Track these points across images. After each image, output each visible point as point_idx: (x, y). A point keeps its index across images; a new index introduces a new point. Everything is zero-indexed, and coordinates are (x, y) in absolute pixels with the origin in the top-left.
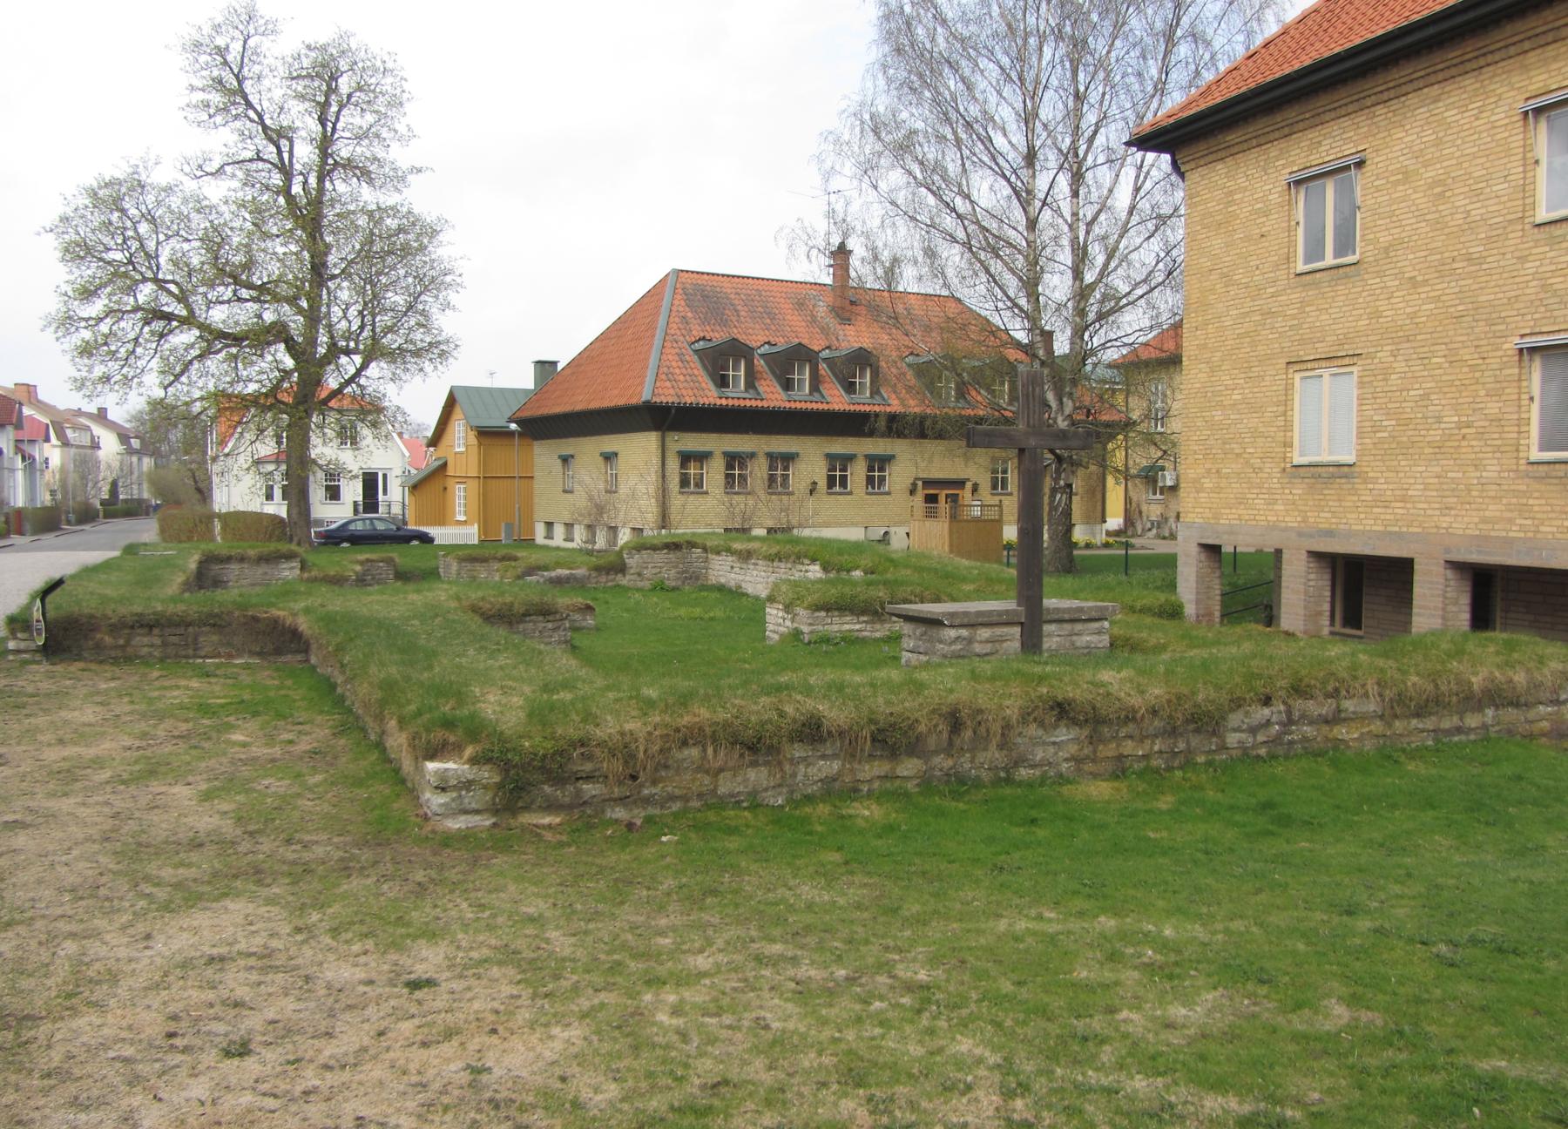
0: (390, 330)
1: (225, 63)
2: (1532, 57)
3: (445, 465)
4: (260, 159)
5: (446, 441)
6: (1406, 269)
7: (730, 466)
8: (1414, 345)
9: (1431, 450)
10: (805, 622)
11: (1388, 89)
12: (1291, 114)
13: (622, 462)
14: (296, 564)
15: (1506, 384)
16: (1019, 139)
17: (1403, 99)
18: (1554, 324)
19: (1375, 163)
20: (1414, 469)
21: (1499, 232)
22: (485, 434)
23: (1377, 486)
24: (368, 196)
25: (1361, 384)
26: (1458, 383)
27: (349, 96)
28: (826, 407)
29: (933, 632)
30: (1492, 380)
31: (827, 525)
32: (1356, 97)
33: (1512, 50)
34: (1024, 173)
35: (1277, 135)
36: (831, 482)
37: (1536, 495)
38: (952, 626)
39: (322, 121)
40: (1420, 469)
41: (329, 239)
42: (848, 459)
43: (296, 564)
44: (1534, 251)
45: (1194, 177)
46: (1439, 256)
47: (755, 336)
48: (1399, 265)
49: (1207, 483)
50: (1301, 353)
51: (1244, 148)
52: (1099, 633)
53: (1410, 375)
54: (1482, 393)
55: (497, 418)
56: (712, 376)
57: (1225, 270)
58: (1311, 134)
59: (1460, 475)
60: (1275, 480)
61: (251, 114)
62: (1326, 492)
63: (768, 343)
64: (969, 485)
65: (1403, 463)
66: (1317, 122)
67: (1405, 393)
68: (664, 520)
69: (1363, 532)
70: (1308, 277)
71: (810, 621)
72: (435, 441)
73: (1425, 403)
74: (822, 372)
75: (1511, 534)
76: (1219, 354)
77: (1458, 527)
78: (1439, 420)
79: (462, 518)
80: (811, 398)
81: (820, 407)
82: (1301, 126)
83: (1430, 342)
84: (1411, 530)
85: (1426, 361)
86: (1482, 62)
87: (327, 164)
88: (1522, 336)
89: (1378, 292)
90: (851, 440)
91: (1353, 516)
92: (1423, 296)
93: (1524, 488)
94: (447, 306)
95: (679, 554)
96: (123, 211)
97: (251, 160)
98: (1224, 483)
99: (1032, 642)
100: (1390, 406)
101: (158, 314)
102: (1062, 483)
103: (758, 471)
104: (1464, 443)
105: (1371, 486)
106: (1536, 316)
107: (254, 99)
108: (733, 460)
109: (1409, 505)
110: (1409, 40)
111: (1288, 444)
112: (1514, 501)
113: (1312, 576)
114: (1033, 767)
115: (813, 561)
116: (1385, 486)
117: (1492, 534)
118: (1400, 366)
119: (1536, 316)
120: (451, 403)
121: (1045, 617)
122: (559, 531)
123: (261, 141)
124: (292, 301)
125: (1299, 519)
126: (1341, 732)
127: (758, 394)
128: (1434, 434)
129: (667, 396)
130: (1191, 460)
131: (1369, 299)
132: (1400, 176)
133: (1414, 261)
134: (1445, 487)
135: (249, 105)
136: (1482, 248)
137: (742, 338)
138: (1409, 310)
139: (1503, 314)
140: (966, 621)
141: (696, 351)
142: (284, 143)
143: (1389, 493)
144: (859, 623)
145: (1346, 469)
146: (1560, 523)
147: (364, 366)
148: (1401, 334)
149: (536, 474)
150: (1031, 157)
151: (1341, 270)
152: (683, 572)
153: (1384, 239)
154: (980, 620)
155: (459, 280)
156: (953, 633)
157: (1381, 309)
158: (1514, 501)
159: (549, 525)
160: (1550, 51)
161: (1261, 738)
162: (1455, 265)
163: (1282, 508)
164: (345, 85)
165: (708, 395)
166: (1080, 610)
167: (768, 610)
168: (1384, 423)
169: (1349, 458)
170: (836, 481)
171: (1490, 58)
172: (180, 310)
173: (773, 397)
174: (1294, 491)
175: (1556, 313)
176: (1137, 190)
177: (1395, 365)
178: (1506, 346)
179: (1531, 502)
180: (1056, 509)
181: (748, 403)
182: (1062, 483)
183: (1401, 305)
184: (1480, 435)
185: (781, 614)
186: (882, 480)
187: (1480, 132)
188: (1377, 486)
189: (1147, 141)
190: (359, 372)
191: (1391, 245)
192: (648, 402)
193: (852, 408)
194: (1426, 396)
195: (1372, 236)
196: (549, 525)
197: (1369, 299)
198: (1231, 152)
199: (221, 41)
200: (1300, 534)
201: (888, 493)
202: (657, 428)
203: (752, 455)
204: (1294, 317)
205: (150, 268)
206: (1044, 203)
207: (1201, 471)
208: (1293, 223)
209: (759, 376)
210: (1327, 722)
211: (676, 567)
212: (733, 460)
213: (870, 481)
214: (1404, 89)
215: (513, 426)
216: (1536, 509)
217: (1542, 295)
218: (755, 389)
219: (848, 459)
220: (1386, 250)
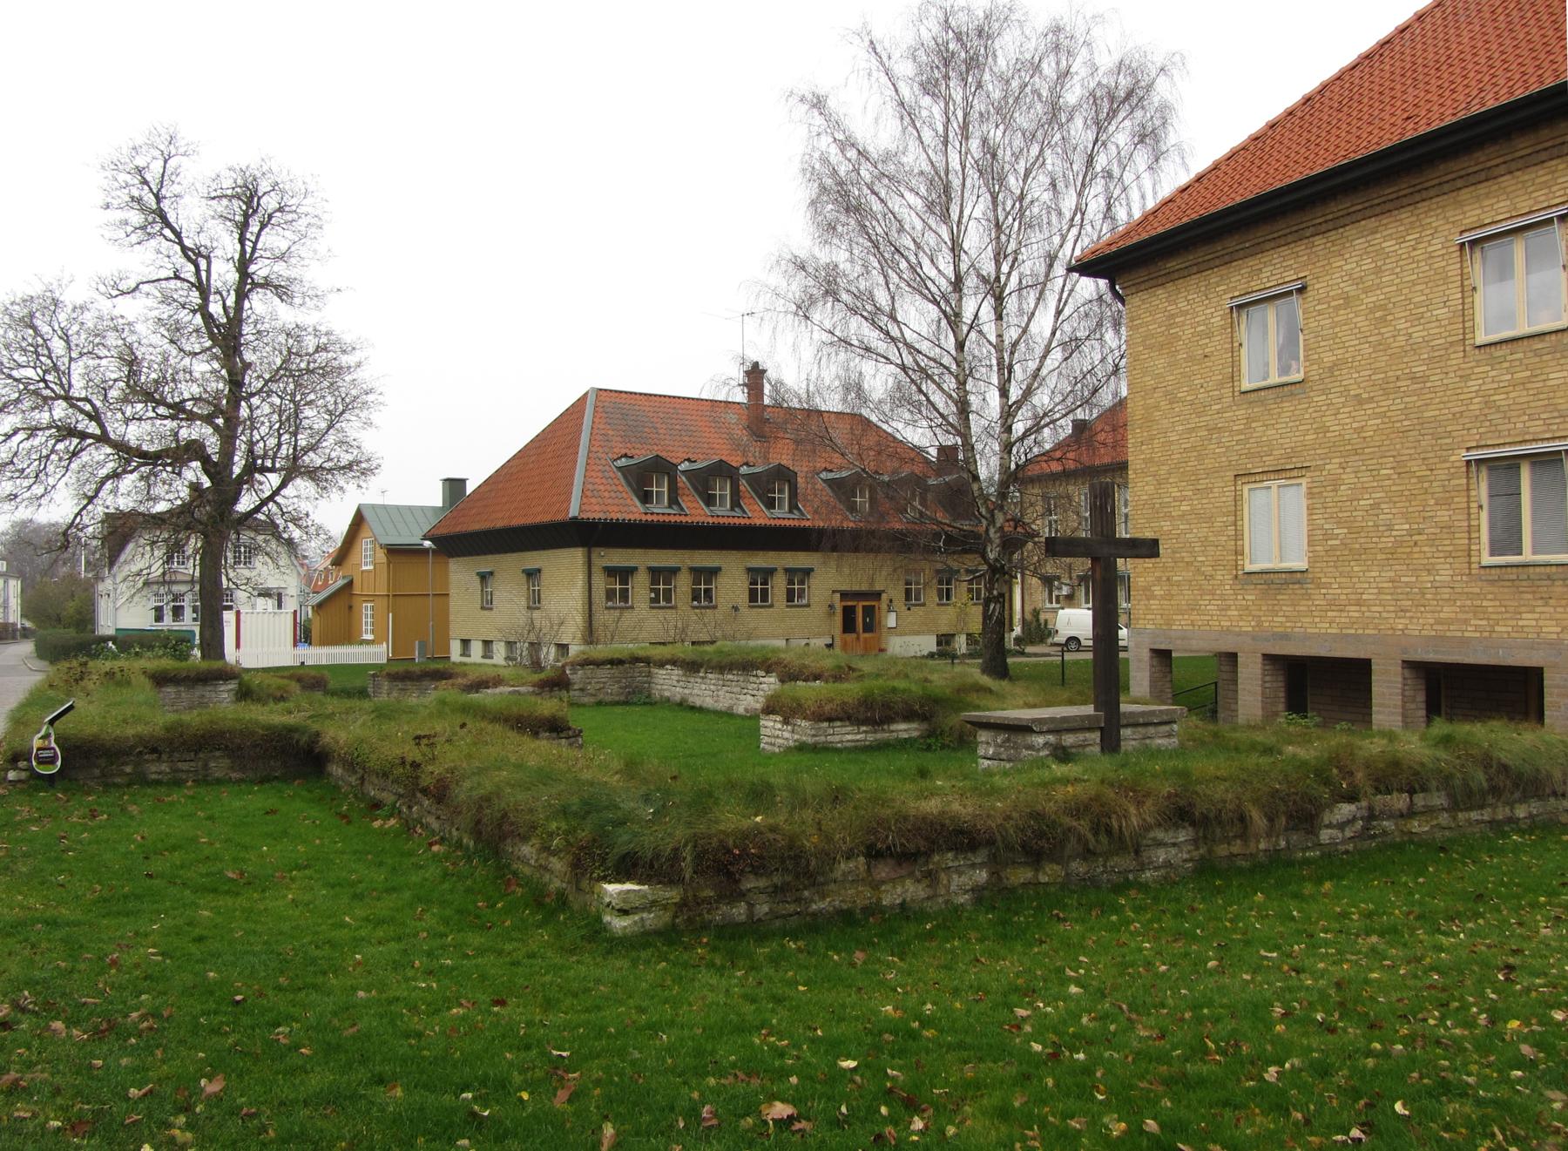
0: (313, 448)
1: (145, 182)
2: (1465, 194)
3: (350, 584)
4: (177, 277)
5: (353, 559)
6: (1351, 387)
7: (655, 581)
8: (1362, 457)
9: (1384, 556)
10: (805, 731)
11: (1326, 222)
12: (1232, 243)
13: (545, 577)
15: (1453, 494)
16: (946, 263)
17: (1341, 230)
18: (1499, 437)
19: (1317, 289)
20: (1367, 574)
21: (1442, 352)
22: (394, 551)
23: (1330, 591)
24: (286, 315)
25: (1310, 494)
26: (1406, 493)
27: (270, 217)
28: (747, 522)
29: (1019, 739)
30: (1441, 489)
31: (767, 637)
32: (1295, 228)
33: (1446, 187)
34: (953, 298)
35: (1217, 262)
36: (753, 596)
37: (1490, 597)
38: (1041, 733)
39: (242, 241)
40: (1373, 574)
41: (249, 356)
42: (770, 572)
44: (1476, 370)
45: (1134, 301)
46: (1383, 376)
47: (675, 453)
48: (1344, 383)
49: (1158, 591)
50: (1249, 466)
51: (1184, 274)
52: (1169, 736)
53: (1359, 485)
54: (1432, 502)
55: (412, 536)
56: (636, 492)
57: (1169, 388)
58: (1251, 262)
59: (1414, 579)
60: (1227, 587)
61: (167, 232)
63: (689, 460)
65: (1356, 569)
66: (1257, 250)
67: (1355, 503)
68: (590, 635)
69: (1319, 635)
70: (1253, 395)
71: (813, 732)
72: (342, 557)
73: (1376, 512)
74: (742, 488)
75: (1466, 634)
76: (1167, 468)
77: (1414, 629)
78: (1390, 528)
79: (370, 637)
80: (733, 514)
81: (743, 521)
82: (1241, 254)
83: (1378, 455)
84: (1367, 632)
85: (1375, 473)
86: (1417, 197)
87: (246, 284)
88: (1468, 449)
89: (1324, 408)
90: (771, 554)
91: (1308, 620)
92: (1368, 412)
93: (1478, 590)
94: (368, 424)
96: (34, 328)
97: (167, 279)
98: (1174, 591)
99: (1110, 743)
100: (1340, 515)
101: (67, 432)
102: (995, 592)
103: (683, 584)
104: (1416, 549)
105: (1323, 591)
106: (1481, 430)
107: (171, 218)
108: (656, 573)
109: (1363, 609)
110: (1349, 177)
111: (1238, 552)
112: (1469, 603)
113: (1268, 678)
114: (1156, 869)
115: (768, 671)
116: (1339, 591)
117: (1448, 634)
118: (1349, 478)
119: (1481, 430)
120: (359, 521)
121: (1124, 721)
122: (477, 649)
123: (180, 260)
124: (208, 419)
126: (1415, 826)
127: (682, 509)
128: (1388, 542)
129: (596, 513)
131: (1314, 415)
132: (1341, 302)
133: (1360, 380)
134: (1399, 591)
135: (169, 225)
136: (1425, 368)
137: (663, 454)
138: (1355, 425)
139: (1449, 429)
140: (1052, 726)
141: (619, 468)
142: (203, 264)
143: (1343, 597)
144: (859, 733)
145: (1299, 575)
146: (1514, 623)
147: (283, 485)
148: (1350, 447)
149: (452, 592)
150: (958, 284)
151: (1286, 388)
152: (626, 687)
153: (1328, 358)
154: (1065, 726)
155: (381, 399)
156: (1040, 740)
157: (1328, 424)
158: (1469, 603)
159: (466, 643)
160: (1482, 189)
161: (1348, 833)
162: (1399, 384)
163: (1236, 613)
164: (269, 203)
165: (631, 510)
166: (1153, 713)
167: (762, 722)
168: (1336, 531)
169: (1302, 565)
170: (758, 596)
171: (1424, 194)
172: (93, 428)
173: (694, 511)
175: (1499, 428)
176: (1059, 312)
177: (1344, 476)
178: (1453, 458)
179: (1485, 603)
180: (990, 618)
181: (673, 519)
182: (995, 592)
183: (1348, 421)
184: (1432, 541)
185: (779, 726)
186: (801, 594)
187: (1418, 262)
188: (1330, 591)
189: (1087, 267)
190: (276, 492)
191: (1335, 365)
192: (575, 518)
193: (773, 523)
194: (1376, 506)
195: (1316, 356)
196: (466, 643)
197: (1314, 415)
198: (1170, 278)
199: (140, 162)
200: (1254, 638)
201: (808, 606)
202: (582, 545)
203: (674, 571)
204: (1240, 432)
205: (62, 385)
206: (971, 327)
208: (1236, 344)
209: (680, 492)
210: (1402, 816)
211: (620, 682)
212: (656, 573)
213: (790, 596)
214: (1342, 221)
215: (427, 544)
216: (1490, 610)
217: (1486, 411)
218: (679, 505)
219: (770, 572)
220: (1331, 369)
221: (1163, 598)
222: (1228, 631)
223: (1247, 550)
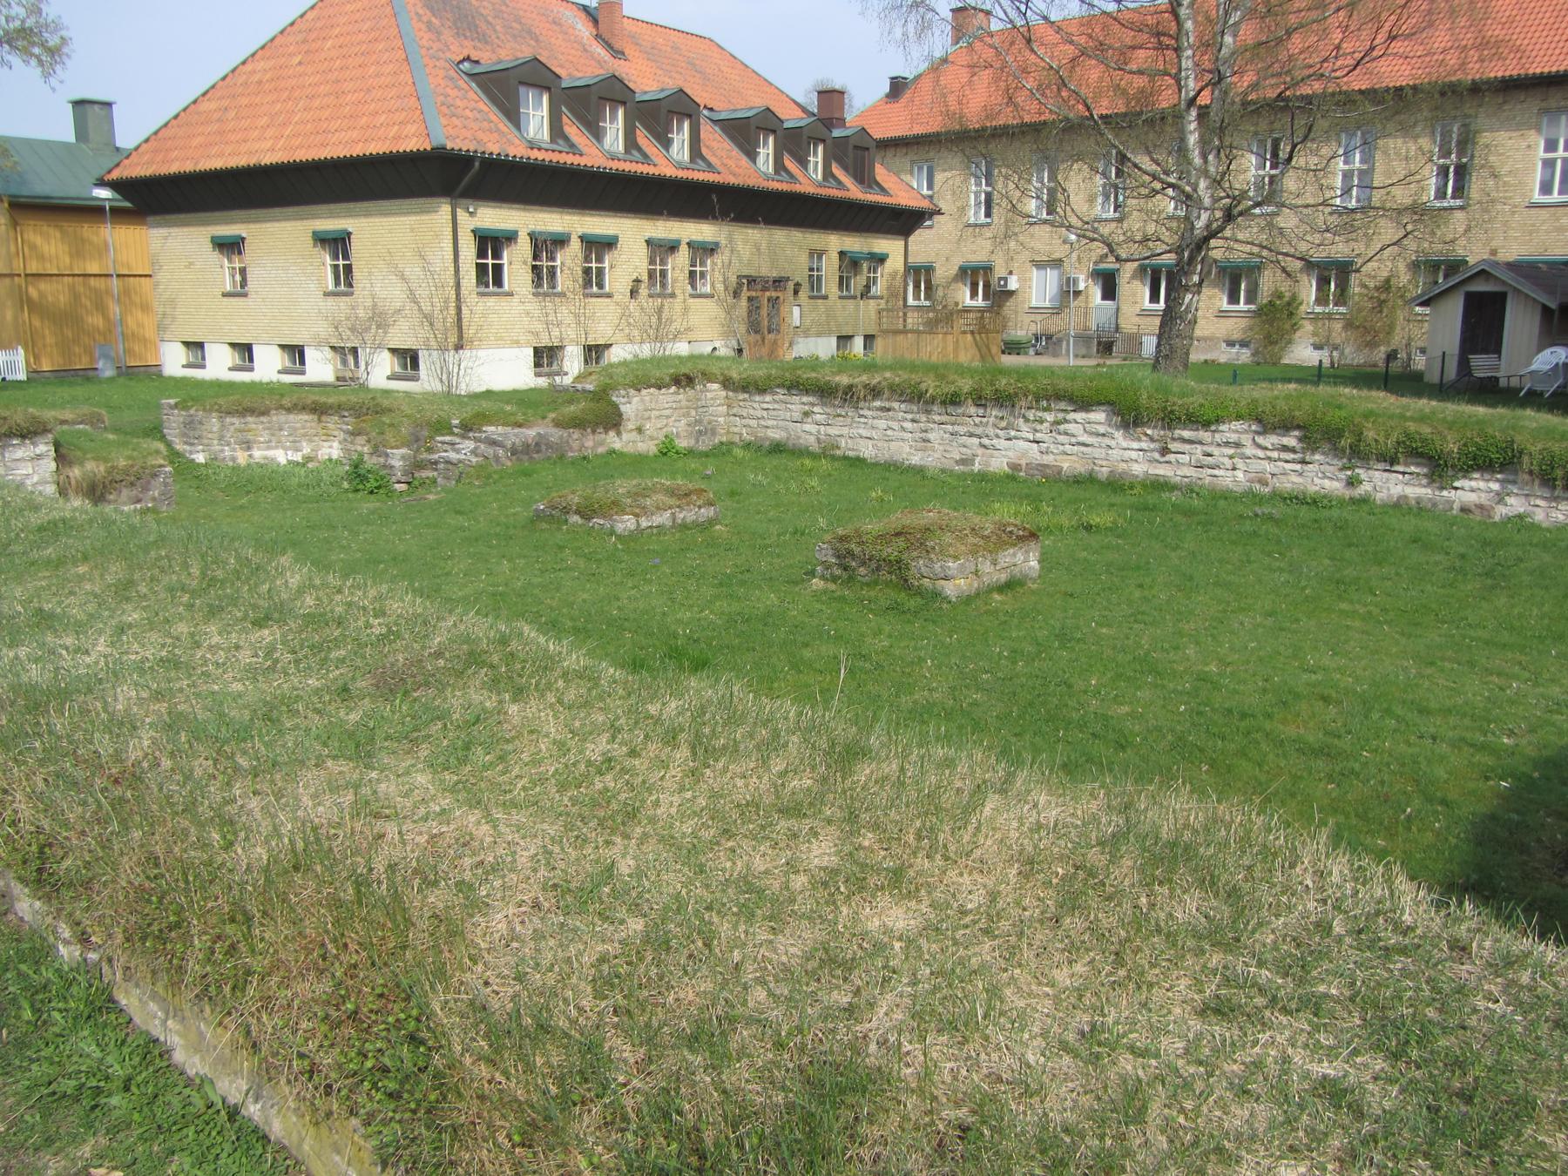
13: (356, 246)
14: (44, 447)
43: (44, 447)
64: (791, 285)
95: (690, 392)
108: (546, 245)
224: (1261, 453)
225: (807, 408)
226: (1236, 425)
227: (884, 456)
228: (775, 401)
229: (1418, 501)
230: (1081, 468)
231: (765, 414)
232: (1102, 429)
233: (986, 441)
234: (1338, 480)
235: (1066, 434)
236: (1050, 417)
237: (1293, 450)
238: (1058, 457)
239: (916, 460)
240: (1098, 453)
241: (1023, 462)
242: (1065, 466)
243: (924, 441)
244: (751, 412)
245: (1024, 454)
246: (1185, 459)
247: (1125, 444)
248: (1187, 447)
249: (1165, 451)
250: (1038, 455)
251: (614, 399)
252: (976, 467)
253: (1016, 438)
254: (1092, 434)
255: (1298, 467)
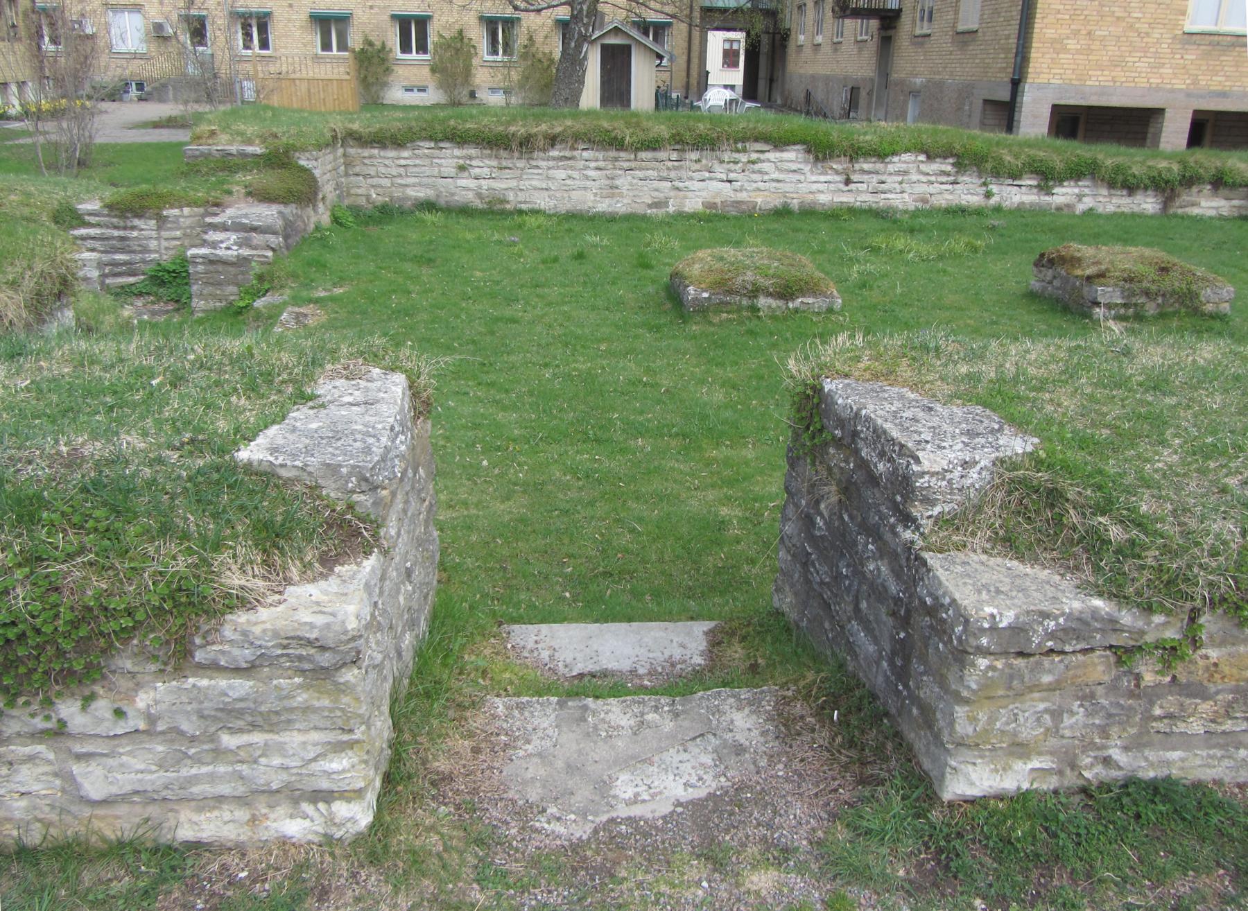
49: (1072, 44)
62: (1223, 58)
125: (1188, 82)
130: (1050, 19)
174: (1186, 57)
200: (1189, 95)
207: (1065, 31)
221: (1078, 52)
222: (1158, 89)
223: (1190, 11)
224: (924, 179)
225: (461, 162)
226: (906, 157)
227: (564, 207)
228: (417, 157)
229: (1031, 204)
230: (776, 202)
231: (402, 171)
232: (794, 166)
233: (677, 184)
234: (977, 195)
235: (760, 172)
236: (743, 158)
237: (948, 174)
238: (752, 194)
239: (603, 206)
240: (787, 187)
241: (718, 201)
242: (759, 200)
243: (611, 187)
244: (382, 170)
245: (718, 194)
246: (863, 187)
247: (814, 178)
248: (865, 178)
249: (848, 182)
250: (732, 194)
251: (302, 163)
252: (671, 209)
253: (711, 179)
254: (781, 171)
255: (949, 187)
